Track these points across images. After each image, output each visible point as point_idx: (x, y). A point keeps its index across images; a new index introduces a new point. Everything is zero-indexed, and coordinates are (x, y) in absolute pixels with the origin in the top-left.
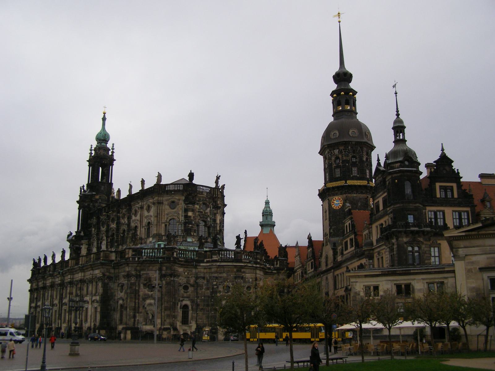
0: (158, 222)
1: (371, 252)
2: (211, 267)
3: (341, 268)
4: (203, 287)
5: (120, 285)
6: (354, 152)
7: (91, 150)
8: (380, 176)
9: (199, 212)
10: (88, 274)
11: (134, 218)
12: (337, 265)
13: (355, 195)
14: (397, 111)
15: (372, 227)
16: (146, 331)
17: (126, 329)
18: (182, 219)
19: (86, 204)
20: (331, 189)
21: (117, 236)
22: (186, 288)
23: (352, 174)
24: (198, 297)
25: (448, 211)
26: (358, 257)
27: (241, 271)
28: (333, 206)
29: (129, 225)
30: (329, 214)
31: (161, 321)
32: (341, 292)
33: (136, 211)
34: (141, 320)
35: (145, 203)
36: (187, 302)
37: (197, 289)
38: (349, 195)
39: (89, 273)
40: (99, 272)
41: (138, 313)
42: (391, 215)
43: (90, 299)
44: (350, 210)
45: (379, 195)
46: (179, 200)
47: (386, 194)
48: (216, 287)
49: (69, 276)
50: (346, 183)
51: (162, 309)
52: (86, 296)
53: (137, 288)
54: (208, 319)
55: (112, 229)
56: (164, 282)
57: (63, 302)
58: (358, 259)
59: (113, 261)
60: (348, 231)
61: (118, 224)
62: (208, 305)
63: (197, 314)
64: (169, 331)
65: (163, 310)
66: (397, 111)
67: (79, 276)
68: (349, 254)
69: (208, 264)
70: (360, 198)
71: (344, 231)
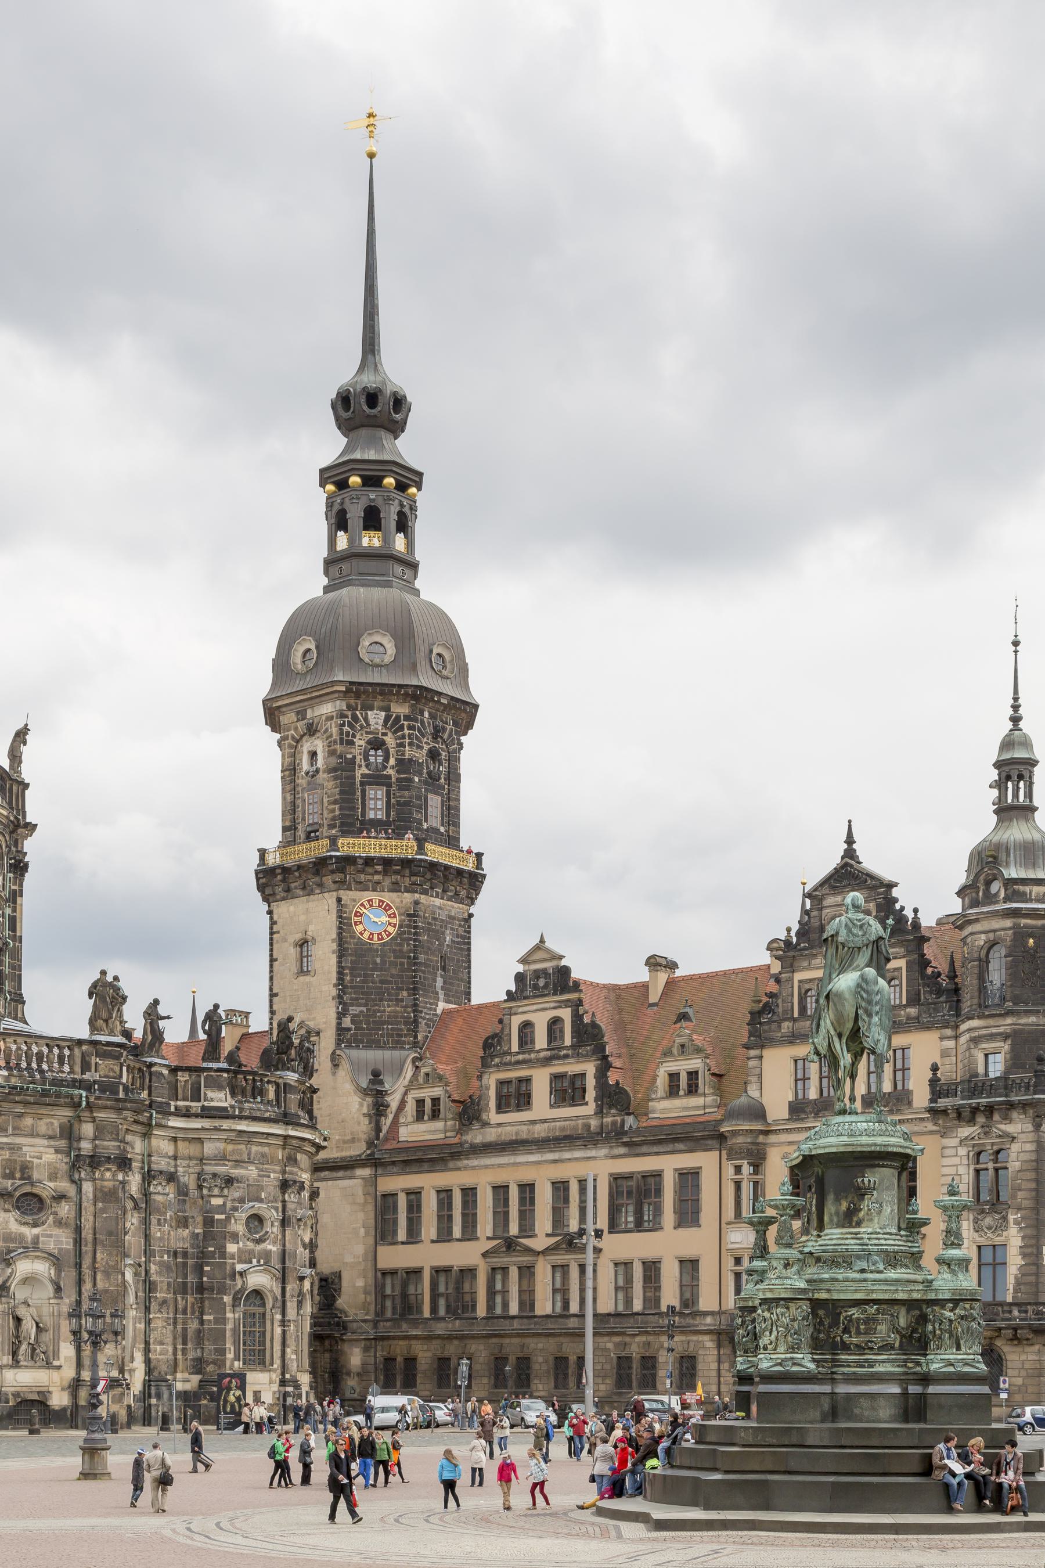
1: (761, 1139)
2: (203, 1135)
3: (458, 1169)
4: (165, 1213)
6: (436, 736)
13: (438, 902)
15: (761, 1057)
20: (360, 861)
23: (426, 821)
24: (148, 1253)
28: (360, 928)
30: (341, 953)
38: (423, 899)
48: (223, 1217)
50: (421, 849)
54: (185, 1343)
58: (622, 1150)
60: (541, 1040)
62: (183, 1289)
63: (148, 1322)
68: (538, 1127)
70: (450, 917)
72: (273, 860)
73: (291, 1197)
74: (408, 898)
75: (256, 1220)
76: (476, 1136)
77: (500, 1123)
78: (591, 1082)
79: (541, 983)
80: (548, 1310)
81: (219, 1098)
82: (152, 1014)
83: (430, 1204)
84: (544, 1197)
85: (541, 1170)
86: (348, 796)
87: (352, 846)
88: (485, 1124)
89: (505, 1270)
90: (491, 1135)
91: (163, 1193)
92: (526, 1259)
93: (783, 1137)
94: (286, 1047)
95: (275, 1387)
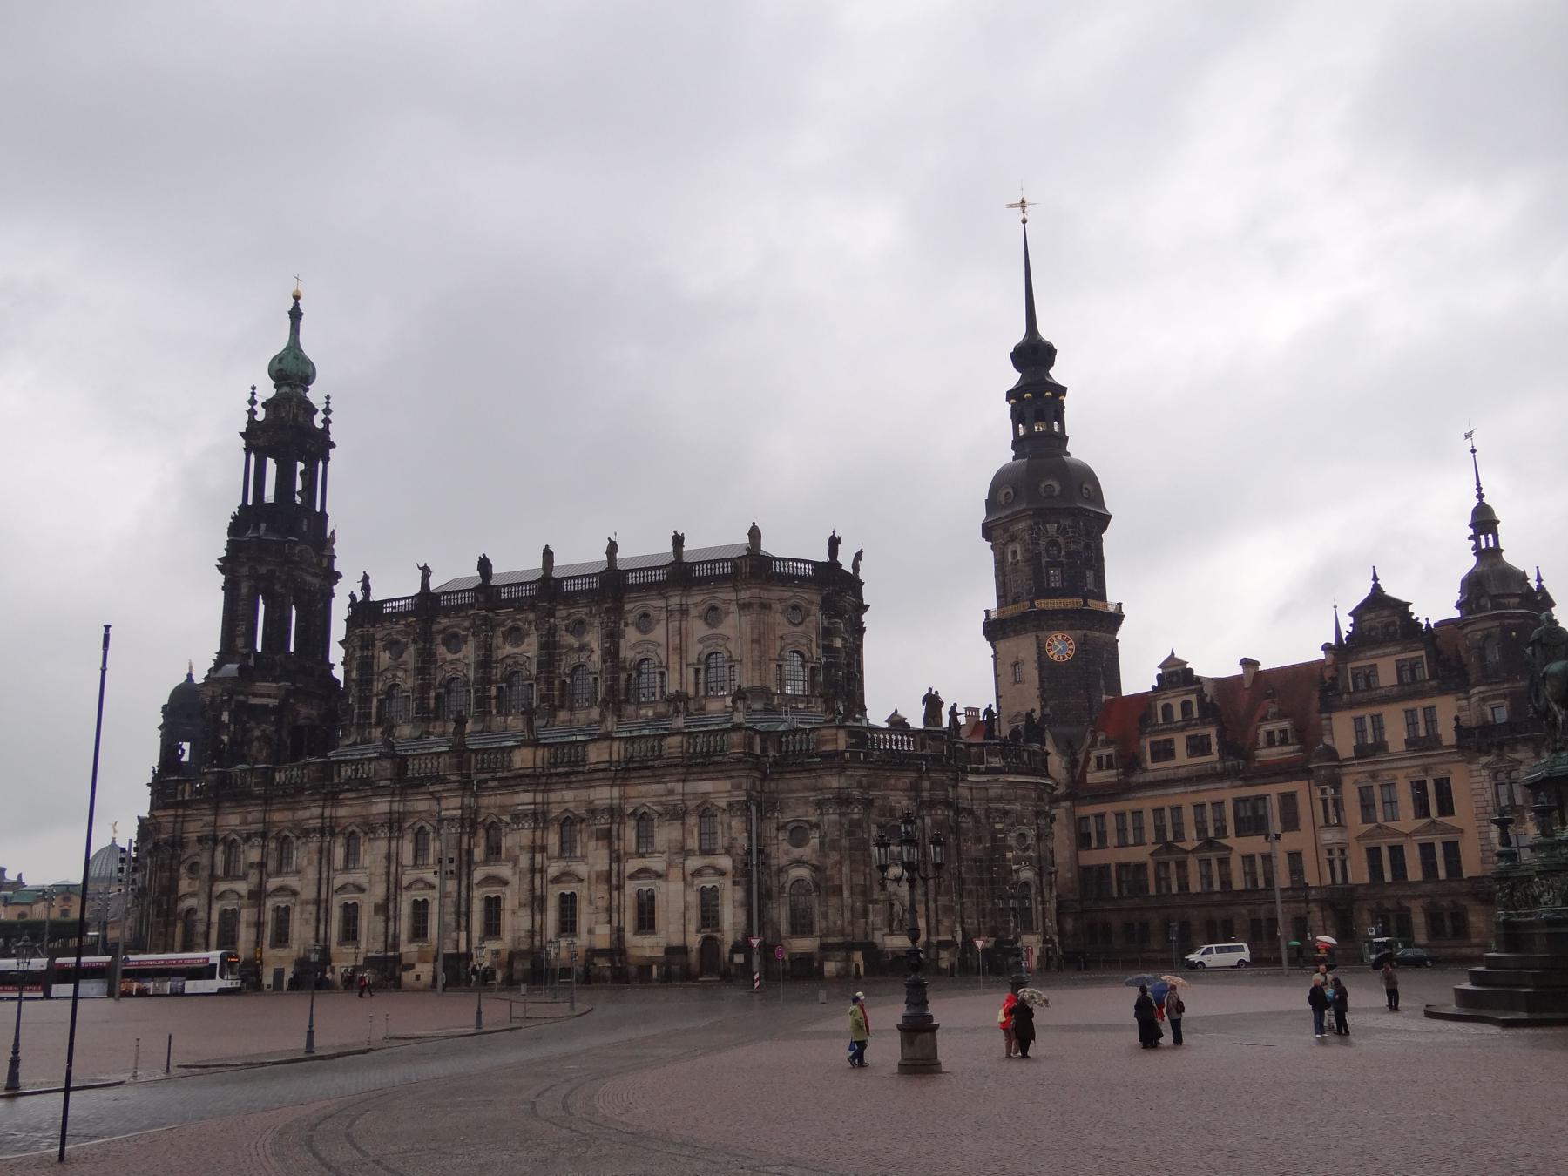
0: (762, 654)
5: (790, 827)
7: (253, 402)
8: (1386, 613)
10: (647, 793)
11: (632, 635)
12: (1078, 791)
14: (1479, 489)
17: (850, 947)
18: (818, 653)
19: (263, 570)
21: (550, 682)
31: (928, 923)
32: (1140, 855)
33: (646, 615)
35: (696, 599)
39: (659, 788)
40: (729, 787)
43: (669, 865)
45: (1380, 652)
46: (811, 603)
47: (1423, 653)
49: (526, 797)
50: (1086, 604)
51: (926, 894)
52: (643, 856)
55: (510, 661)
57: (478, 874)
59: (757, 757)
60: (1178, 715)
61: (549, 648)
62: (981, 882)
63: (962, 904)
65: (931, 895)
66: (1479, 489)
67: (603, 795)
69: (984, 778)
72: (993, 616)
73: (1041, 822)
74: (1079, 632)
75: (1023, 836)
76: (1139, 778)
77: (1155, 769)
78: (1214, 740)
80: (1199, 889)
81: (996, 762)
82: (953, 713)
83: (1111, 824)
84: (1188, 815)
85: (1186, 798)
86: (1038, 575)
87: (1041, 604)
88: (1146, 770)
89: (1166, 865)
90: (1149, 777)
91: (966, 822)
92: (1180, 856)
93: (1352, 769)
94: (1033, 729)
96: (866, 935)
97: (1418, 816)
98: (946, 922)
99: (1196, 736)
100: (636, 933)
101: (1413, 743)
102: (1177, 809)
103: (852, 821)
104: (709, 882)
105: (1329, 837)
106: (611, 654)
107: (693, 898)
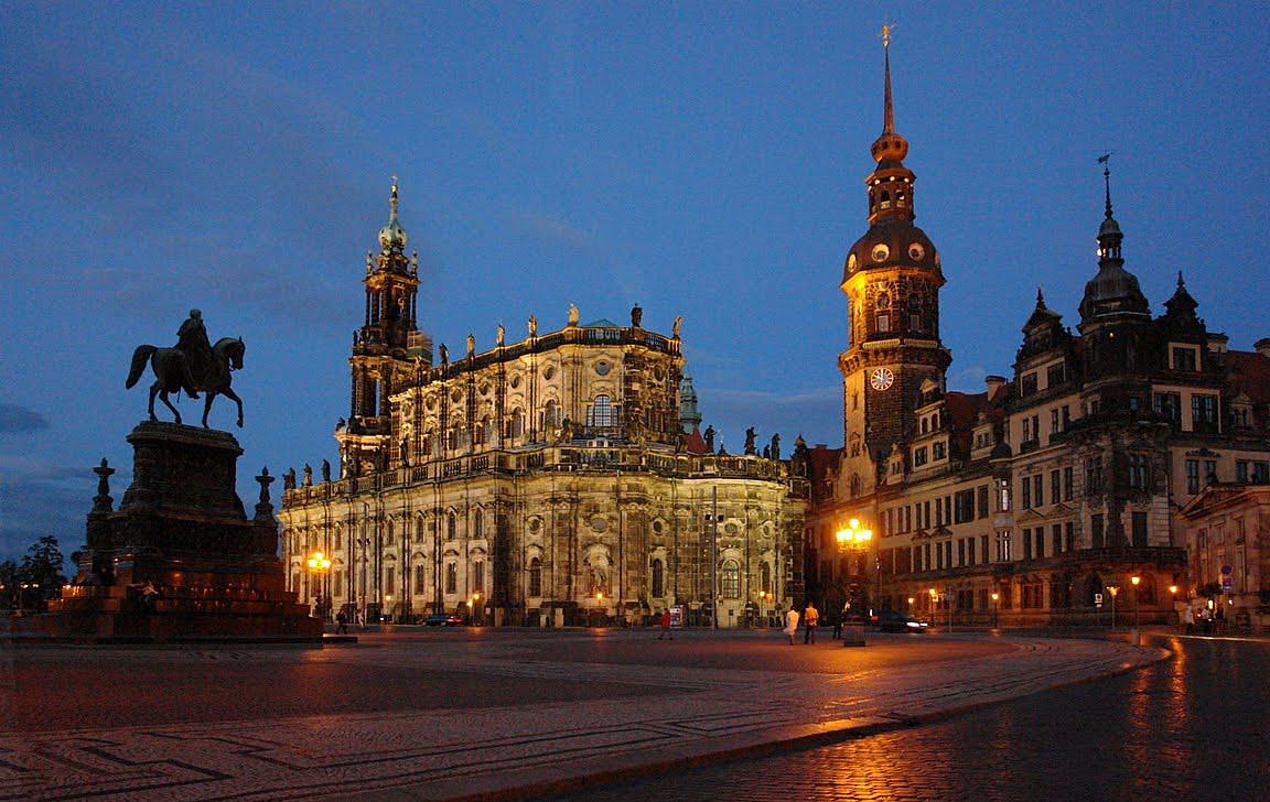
1: (1009, 465)
3: (909, 495)
9: (649, 383)
13: (915, 366)
15: (1008, 421)
16: (591, 610)
22: (658, 527)
24: (677, 544)
25: (1186, 393)
26: (961, 476)
27: (756, 497)
29: (500, 406)
34: (581, 587)
36: (660, 553)
37: (675, 530)
39: (459, 493)
41: (576, 573)
42: (1097, 397)
44: (935, 389)
53: (573, 526)
56: (625, 514)
57: (384, 554)
58: (959, 479)
60: (930, 428)
62: (695, 561)
64: (636, 609)
65: (624, 568)
68: (930, 471)
71: (916, 428)
73: (753, 514)
76: (912, 478)
78: (947, 444)
79: (930, 397)
84: (933, 506)
93: (1019, 464)
95: (743, 608)
96: (569, 597)
97: (1054, 503)
98: (634, 589)
99: (938, 443)
100: (447, 593)
101: (1053, 438)
102: (927, 504)
103: (560, 514)
104: (478, 558)
105: (1000, 521)
106: (500, 406)
107: (471, 569)
